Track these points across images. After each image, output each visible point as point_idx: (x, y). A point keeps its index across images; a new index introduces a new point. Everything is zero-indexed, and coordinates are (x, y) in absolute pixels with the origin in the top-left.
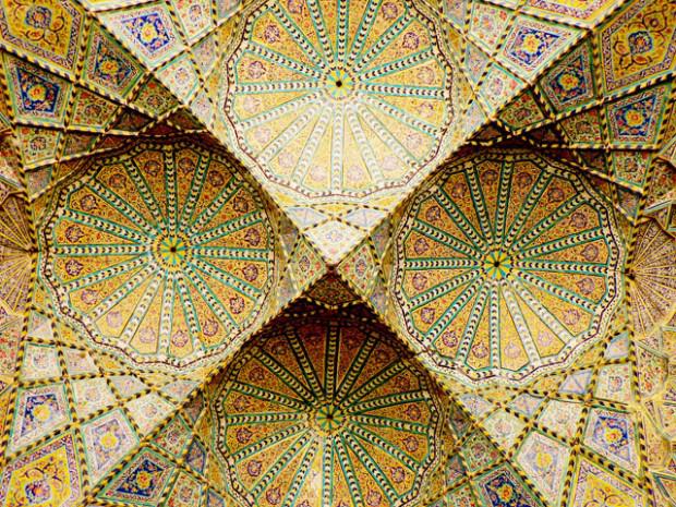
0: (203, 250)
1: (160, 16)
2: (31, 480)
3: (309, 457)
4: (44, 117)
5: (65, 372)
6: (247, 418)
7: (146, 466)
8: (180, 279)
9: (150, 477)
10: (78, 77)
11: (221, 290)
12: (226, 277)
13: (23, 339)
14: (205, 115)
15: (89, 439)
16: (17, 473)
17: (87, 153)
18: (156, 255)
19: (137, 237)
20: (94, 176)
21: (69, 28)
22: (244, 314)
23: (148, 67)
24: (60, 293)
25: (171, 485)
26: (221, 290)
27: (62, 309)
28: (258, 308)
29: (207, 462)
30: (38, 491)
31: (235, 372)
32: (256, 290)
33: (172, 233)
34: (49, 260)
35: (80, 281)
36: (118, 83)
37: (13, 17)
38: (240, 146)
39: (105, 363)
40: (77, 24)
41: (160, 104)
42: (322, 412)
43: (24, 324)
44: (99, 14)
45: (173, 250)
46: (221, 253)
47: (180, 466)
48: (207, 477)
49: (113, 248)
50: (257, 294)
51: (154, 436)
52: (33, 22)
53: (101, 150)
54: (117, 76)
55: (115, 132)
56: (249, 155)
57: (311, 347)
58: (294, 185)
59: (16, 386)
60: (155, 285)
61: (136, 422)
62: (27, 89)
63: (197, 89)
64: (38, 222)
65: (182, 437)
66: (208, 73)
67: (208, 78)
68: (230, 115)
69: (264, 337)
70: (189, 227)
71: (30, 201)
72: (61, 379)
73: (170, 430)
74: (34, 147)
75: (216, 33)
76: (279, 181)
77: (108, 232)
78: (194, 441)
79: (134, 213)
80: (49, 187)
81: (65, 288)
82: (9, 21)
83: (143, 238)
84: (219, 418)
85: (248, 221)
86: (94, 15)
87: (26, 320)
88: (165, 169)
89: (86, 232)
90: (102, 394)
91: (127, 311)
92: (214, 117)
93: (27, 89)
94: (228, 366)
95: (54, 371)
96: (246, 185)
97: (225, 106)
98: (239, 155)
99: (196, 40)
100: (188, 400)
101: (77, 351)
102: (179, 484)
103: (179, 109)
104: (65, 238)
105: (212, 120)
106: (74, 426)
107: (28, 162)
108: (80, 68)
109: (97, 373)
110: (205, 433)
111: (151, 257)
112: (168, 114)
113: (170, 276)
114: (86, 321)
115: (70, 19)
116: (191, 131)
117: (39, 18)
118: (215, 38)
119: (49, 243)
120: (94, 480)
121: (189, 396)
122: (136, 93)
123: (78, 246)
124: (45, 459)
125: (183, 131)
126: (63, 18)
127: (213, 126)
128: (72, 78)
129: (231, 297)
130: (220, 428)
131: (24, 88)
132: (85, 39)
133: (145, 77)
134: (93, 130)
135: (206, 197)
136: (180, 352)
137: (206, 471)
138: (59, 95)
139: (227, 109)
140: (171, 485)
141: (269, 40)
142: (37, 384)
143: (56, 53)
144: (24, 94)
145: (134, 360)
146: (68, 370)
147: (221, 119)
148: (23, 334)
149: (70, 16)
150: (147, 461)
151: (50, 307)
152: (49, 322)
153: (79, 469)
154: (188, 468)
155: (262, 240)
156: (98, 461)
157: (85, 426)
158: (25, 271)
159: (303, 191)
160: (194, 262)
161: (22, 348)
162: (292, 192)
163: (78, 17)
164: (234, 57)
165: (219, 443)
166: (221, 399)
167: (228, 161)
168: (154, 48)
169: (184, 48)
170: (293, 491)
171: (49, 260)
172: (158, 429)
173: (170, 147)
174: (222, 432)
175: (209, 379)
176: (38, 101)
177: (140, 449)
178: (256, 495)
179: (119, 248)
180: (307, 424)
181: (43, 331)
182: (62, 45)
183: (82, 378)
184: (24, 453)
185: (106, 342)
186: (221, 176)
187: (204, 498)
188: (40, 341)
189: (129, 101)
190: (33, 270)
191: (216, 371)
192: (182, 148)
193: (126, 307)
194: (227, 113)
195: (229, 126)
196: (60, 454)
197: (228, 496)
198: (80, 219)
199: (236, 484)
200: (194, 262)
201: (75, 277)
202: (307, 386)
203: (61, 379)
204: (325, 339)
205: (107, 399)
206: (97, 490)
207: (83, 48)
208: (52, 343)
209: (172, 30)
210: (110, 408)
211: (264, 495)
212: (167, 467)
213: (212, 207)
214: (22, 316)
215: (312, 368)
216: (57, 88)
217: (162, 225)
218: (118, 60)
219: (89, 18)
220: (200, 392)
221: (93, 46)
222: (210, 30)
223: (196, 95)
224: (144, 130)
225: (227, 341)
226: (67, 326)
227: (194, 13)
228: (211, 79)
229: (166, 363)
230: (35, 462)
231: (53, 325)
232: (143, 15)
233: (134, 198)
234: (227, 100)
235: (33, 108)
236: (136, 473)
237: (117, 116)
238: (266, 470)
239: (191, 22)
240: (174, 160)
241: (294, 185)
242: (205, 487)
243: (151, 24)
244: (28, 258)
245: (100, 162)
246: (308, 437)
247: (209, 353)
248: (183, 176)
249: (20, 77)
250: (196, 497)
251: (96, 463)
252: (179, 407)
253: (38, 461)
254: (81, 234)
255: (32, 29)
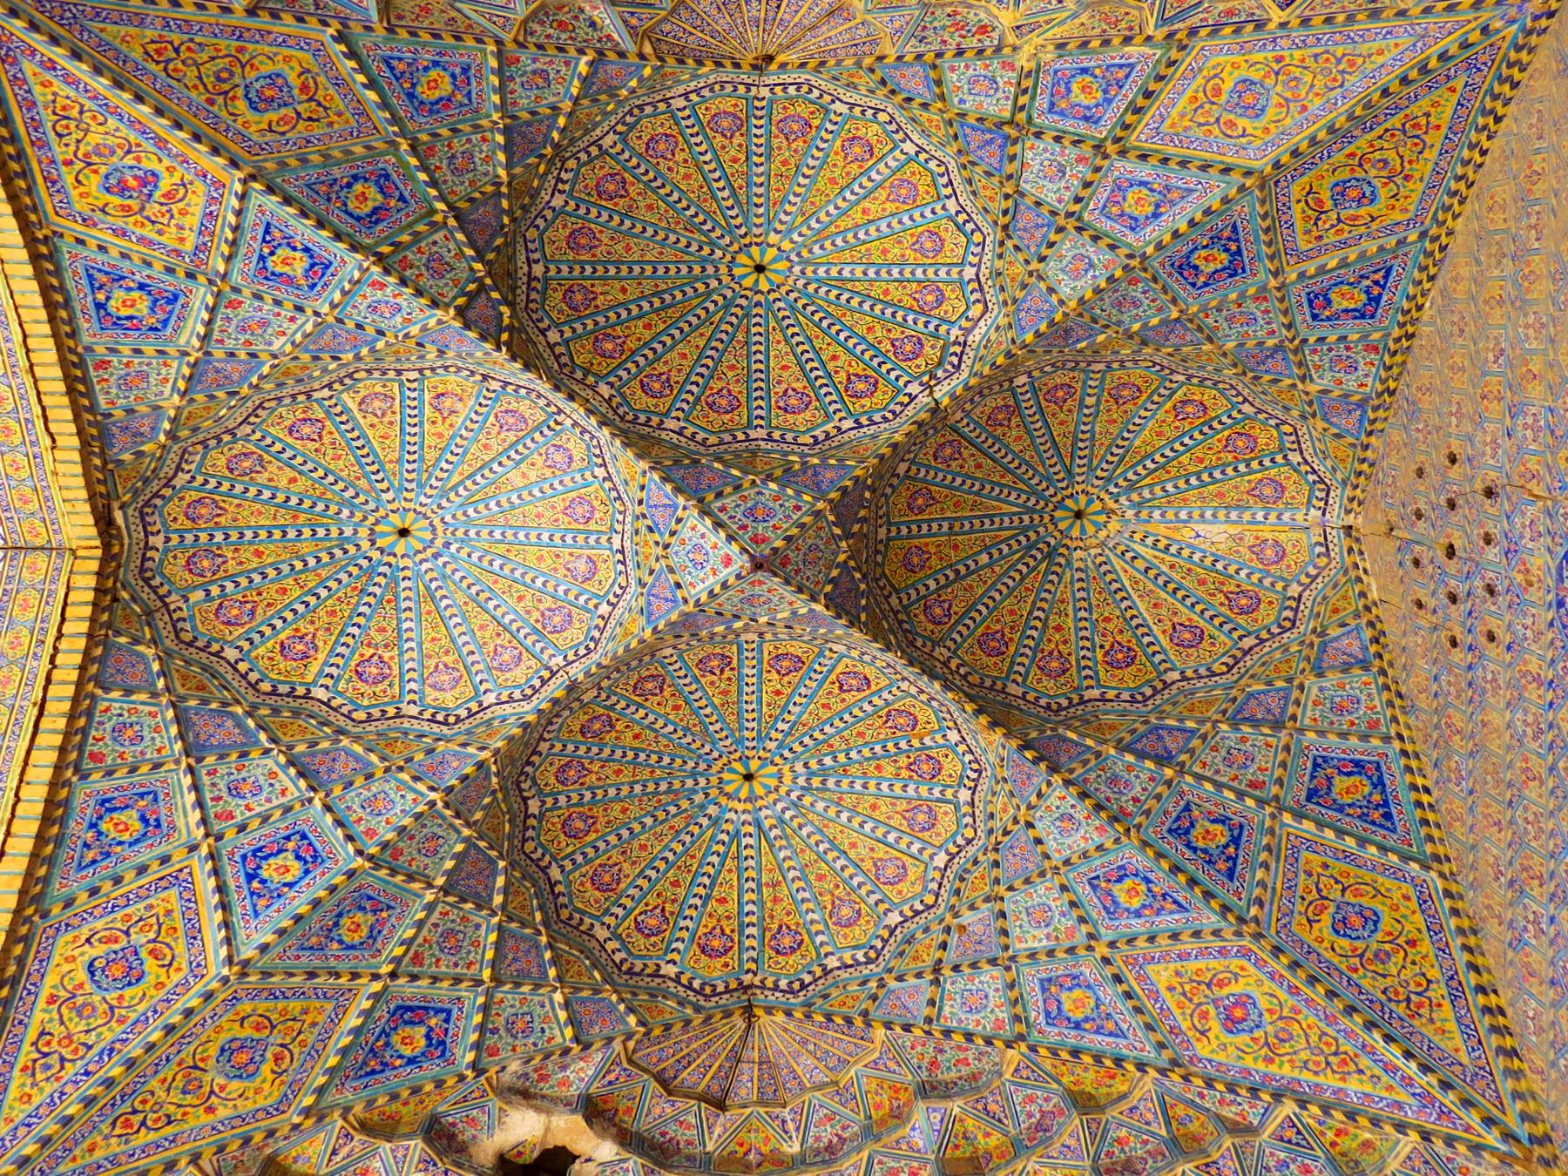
0: (747, 734)
1: (247, 849)
2: (1215, 1025)
3: (1161, 545)
4: (461, 1024)
5: (993, 962)
6: (1084, 652)
7: (1181, 831)
8: (806, 765)
9: (1203, 825)
10: (376, 977)
11: (824, 706)
12: (797, 699)
13: (928, 1033)
14: (460, 762)
15: (1128, 926)
16: (1202, 1049)
17: (544, 939)
18: (760, 803)
19: (724, 837)
20: (597, 918)
21: (262, 1006)
22: (870, 672)
23: (353, 865)
24: (838, 964)
25: (1219, 786)
26: (824, 706)
27: (869, 961)
28: (855, 654)
29: (1169, 722)
30: (1238, 1013)
31: (988, 683)
32: (821, 654)
33: (714, 780)
34: (769, 984)
35: (814, 928)
36: (389, 907)
37: (239, 1102)
38: (526, 698)
39: (978, 887)
40: (255, 995)
41: (436, 837)
42: (1071, 527)
43: (898, 1030)
44: (236, 960)
45: (749, 777)
46: (750, 707)
47: (1182, 772)
48: (1201, 722)
49: (746, 875)
50: (827, 653)
51: (1116, 819)
52: (252, 1068)
53: (538, 916)
54: (375, 912)
55: (498, 899)
56: (544, 682)
57: (934, 562)
58: (604, 609)
59: (1023, 1047)
60: (820, 806)
61: (1091, 846)
62: (400, 1057)
63: (405, 776)
64: (689, 1011)
65: (1119, 768)
66: (373, 758)
67: (383, 759)
68: (463, 713)
69: (912, 643)
70: (700, 757)
71: (642, 1029)
72: (1008, 969)
73: (1106, 792)
74: (528, 1031)
75: (290, 747)
76: (596, 634)
77: (713, 884)
78: (1128, 749)
79: (674, 845)
80: (614, 998)
81: (826, 955)
82: (245, 1107)
83: (725, 827)
84: (1082, 702)
85: (682, 673)
86: (236, 969)
87: (888, 1026)
88: (580, 804)
89: (714, 922)
90: (1037, 900)
91: (872, 850)
92: (464, 745)
93: (400, 1057)
94: (972, 699)
95: (990, 979)
96: (605, 683)
97: (446, 723)
98: (541, 701)
99: (302, 784)
100: (1043, 766)
101: (953, 940)
102: (1217, 772)
103: (447, 805)
104: (723, 960)
105: (471, 750)
106: (1102, 950)
107: (559, 1040)
108: (355, 976)
109: (997, 906)
110: (1112, 728)
111: (764, 812)
112: (458, 822)
113: (801, 781)
114: (894, 918)
115: (246, 1007)
116: (494, 780)
117: (243, 1057)
118: (301, 748)
119: (733, 985)
120: (1211, 920)
121: (1036, 761)
122: (411, 878)
123: (741, 933)
124: (1170, 1001)
125: (494, 792)
126: (243, 1019)
127: (482, 749)
128: (376, 986)
129: (837, 691)
130: (1103, 700)
131: (398, 1062)
132: (292, 975)
133: (377, 867)
134: (493, 937)
135: (636, 737)
136: (951, 767)
137: (1190, 724)
138: (416, 1003)
139: (452, 720)
140: (1219, 786)
141: (312, 652)
142: (1019, 1009)
143: (320, 1019)
144: (411, 1061)
145: (969, 842)
146: (991, 955)
147: (469, 732)
148: (917, 1032)
149: (239, 1007)
150: (1170, 831)
151: (864, 983)
152: (893, 984)
153: (1188, 944)
154: (1183, 757)
155: (718, 650)
156: (1172, 912)
157: (1103, 931)
158: (791, 1027)
159: (616, 596)
160: (772, 745)
161: (947, 1033)
162: (618, 611)
163: (242, 994)
164: (345, 710)
165: (1133, 700)
166: (1043, 702)
167: (557, 716)
168: (315, 857)
169: (317, 803)
170: (1231, 570)
171: (769, 984)
172: (1103, 815)
173: (534, 805)
174: (1111, 694)
175: (1000, 731)
176: (428, 1037)
177: (1145, 844)
178: (1241, 632)
179: (745, 864)
180: (1093, 552)
181: (914, 995)
182: (305, 1012)
183: (1005, 933)
184: (1160, 1037)
185: (934, 886)
186: (590, 721)
187: (1246, 729)
188: (932, 1003)
189: (430, 886)
190: (789, 1014)
191: (984, 720)
192: (535, 782)
193: (864, 852)
194: (458, 720)
195: (489, 714)
196: (1161, 975)
197: (1242, 682)
198: (685, 935)
199: (1216, 667)
200: (772, 745)
201: (806, 937)
202: (1016, 557)
203: (1008, 969)
204: (916, 542)
205: (1044, 893)
206: (1231, 918)
207: (312, 975)
208: (936, 982)
209: (279, 826)
210: (1064, 888)
211: (1241, 620)
212: (1182, 794)
213: (657, 726)
214: (880, 1033)
215: (980, 552)
216: (399, 1008)
217: (699, 798)
218: (340, 915)
219: (244, 975)
220: (1026, 746)
221: (308, 960)
222: (282, 759)
223: (416, 779)
224: (494, 853)
225: (924, 697)
226: (901, 954)
227: (245, 789)
228: (388, 751)
229: (974, 790)
230: (1180, 1018)
231: (900, 979)
232: (242, 880)
233: (643, 847)
234: (432, 720)
235: (443, 1043)
236: (1195, 850)
237: (464, 901)
238: (1185, 614)
239: (264, 795)
240: (559, 793)
241: (604, 609)
242: (1224, 727)
243: (264, 864)
244: (763, 1019)
245: (565, 914)
246: (1122, 548)
247: (951, 724)
248: (594, 777)
249: (373, 1072)
250: (1243, 740)
251: (1176, 916)
252: (1057, 779)
253: (1177, 1012)
254: (718, 930)
255: (266, 1069)
